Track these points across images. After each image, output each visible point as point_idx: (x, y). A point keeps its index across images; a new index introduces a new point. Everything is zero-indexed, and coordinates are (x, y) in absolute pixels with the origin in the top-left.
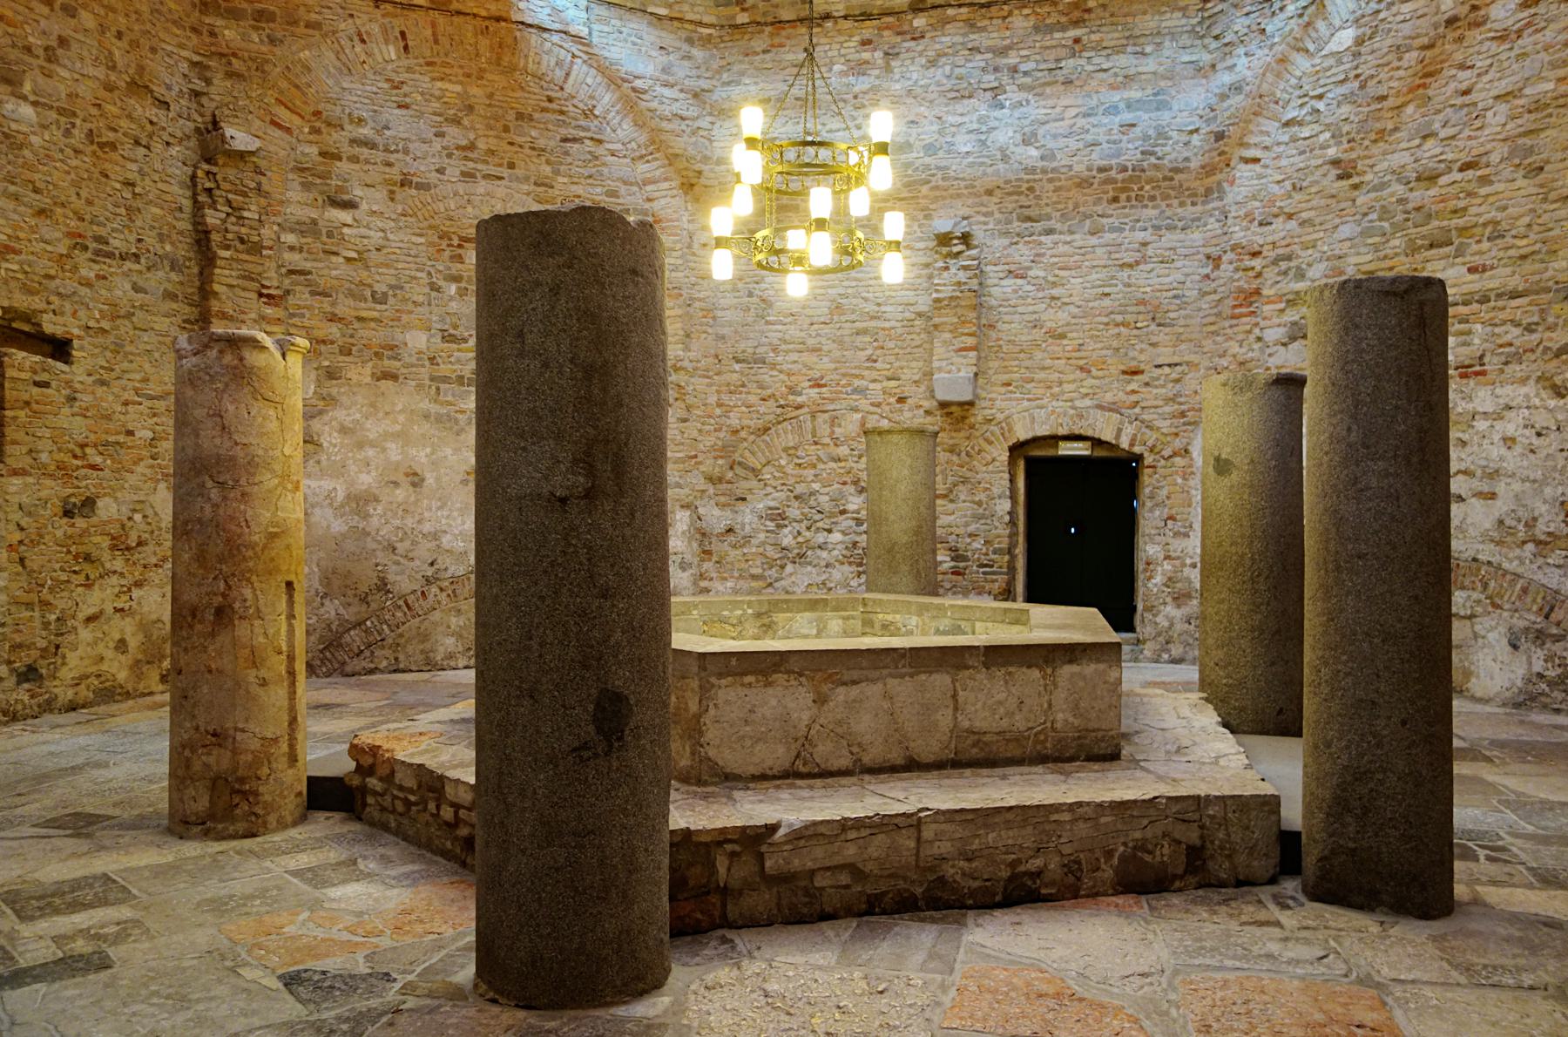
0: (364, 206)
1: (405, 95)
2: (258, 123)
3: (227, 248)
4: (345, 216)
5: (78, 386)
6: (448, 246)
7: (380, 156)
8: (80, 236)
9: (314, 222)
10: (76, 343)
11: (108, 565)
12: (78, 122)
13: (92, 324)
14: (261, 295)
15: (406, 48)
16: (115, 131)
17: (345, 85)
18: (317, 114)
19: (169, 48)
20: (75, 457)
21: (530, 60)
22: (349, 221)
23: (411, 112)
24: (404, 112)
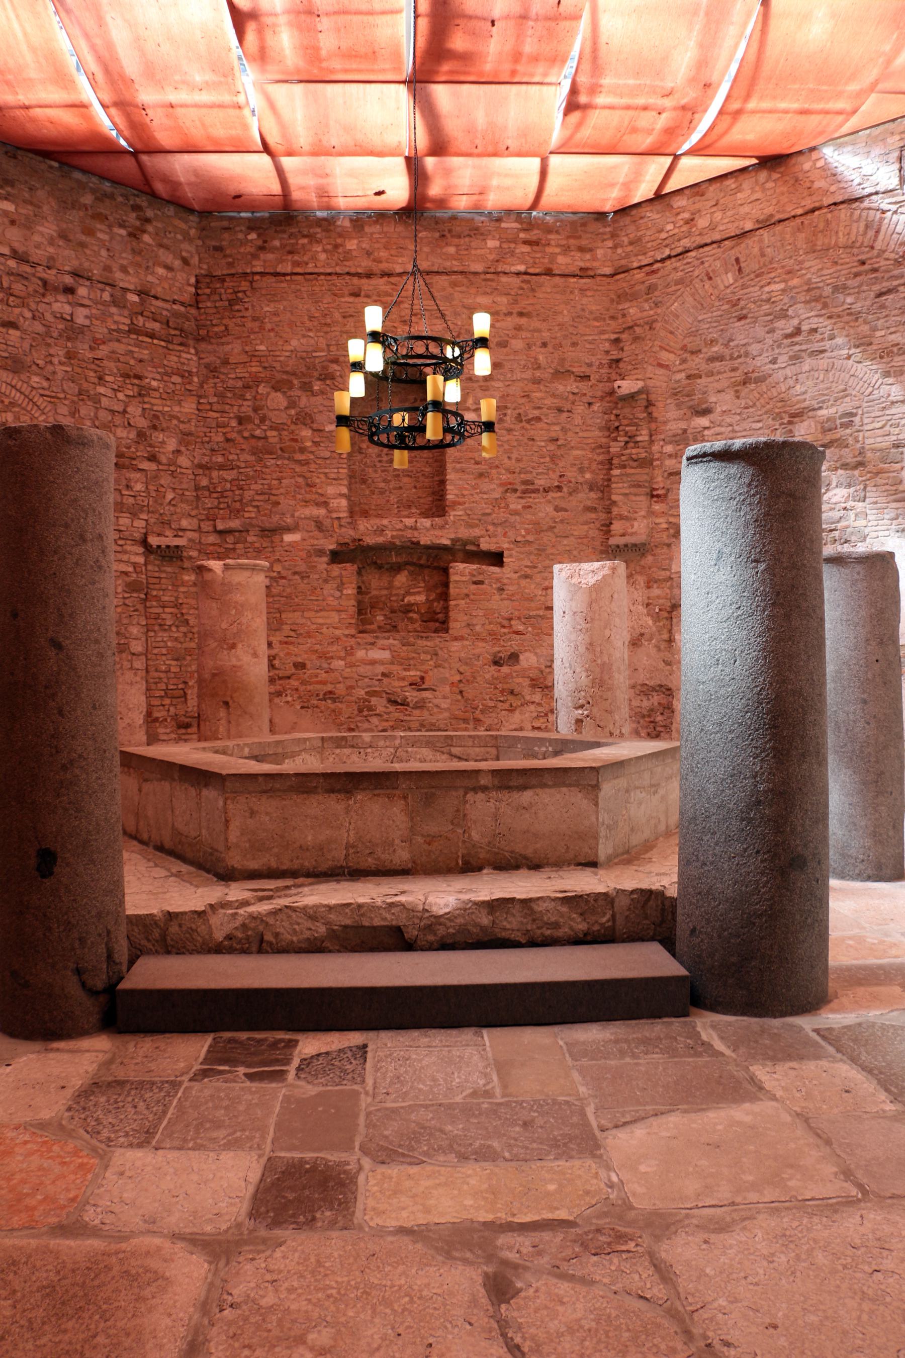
0: (719, 409)
1: (742, 309)
2: (650, 368)
3: (624, 467)
4: (704, 421)
5: (505, 581)
6: (781, 424)
7: (728, 364)
8: (510, 484)
9: (685, 431)
10: (506, 554)
11: (528, 698)
12: (509, 412)
13: (518, 539)
14: (653, 496)
15: (740, 270)
16: (539, 408)
17: (700, 318)
18: (684, 348)
19: (590, 338)
20: (504, 627)
21: (841, 234)
22: (707, 424)
23: (748, 321)
24: (742, 322)
